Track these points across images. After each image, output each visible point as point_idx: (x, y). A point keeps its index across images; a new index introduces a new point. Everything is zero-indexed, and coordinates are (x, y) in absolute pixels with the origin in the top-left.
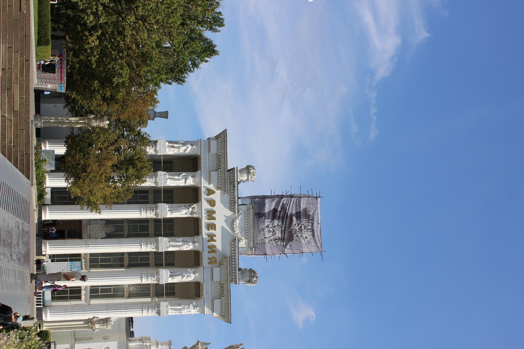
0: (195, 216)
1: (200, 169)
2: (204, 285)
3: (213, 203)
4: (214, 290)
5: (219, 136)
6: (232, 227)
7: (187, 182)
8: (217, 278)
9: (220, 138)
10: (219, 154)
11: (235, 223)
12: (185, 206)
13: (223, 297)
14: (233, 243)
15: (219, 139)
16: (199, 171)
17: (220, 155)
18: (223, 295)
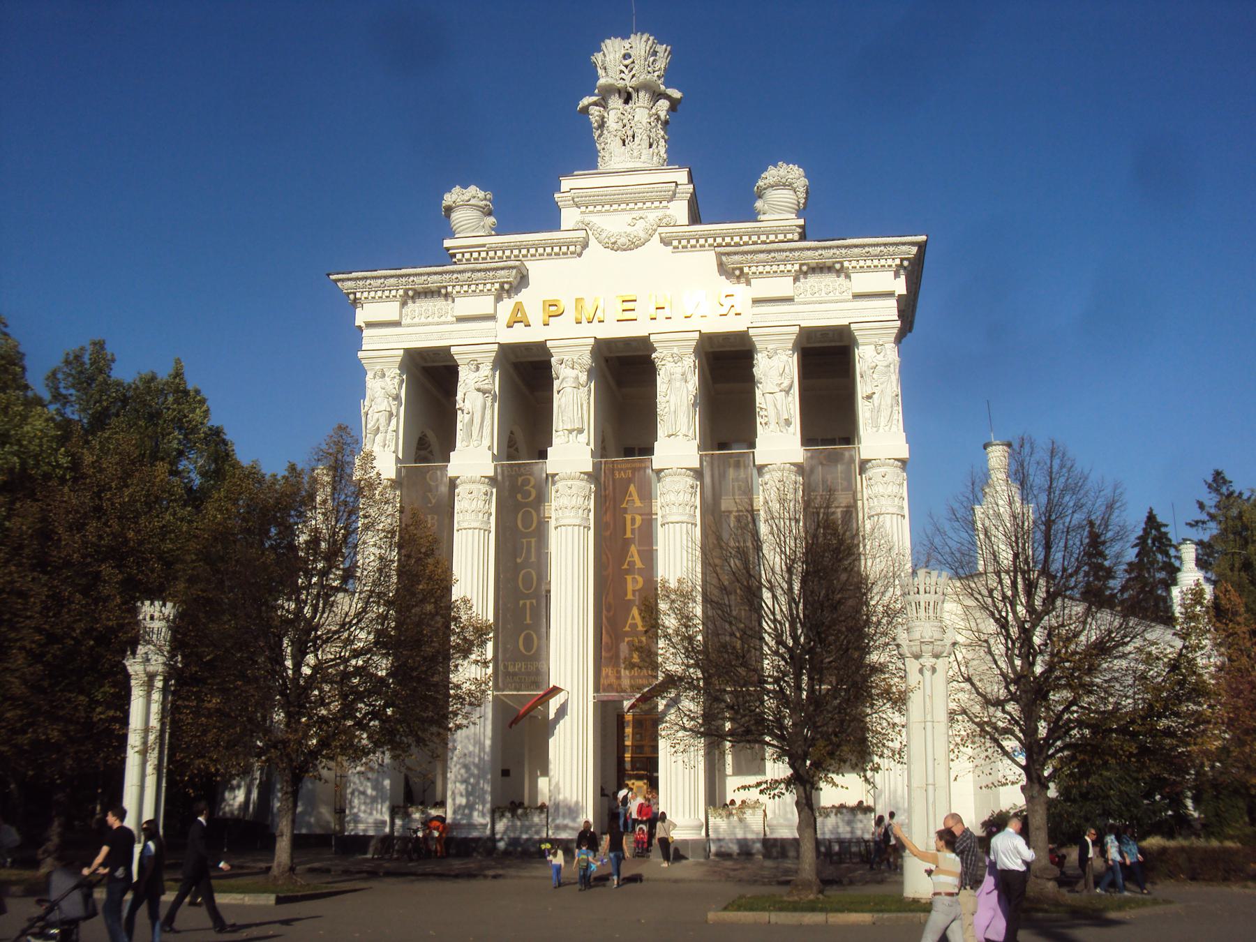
0: (587, 360)
1: (447, 350)
2: (804, 324)
3: (552, 308)
4: (823, 294)
5: (352, 296)
6: (625, 250)
7: (486, 387)
8: (782, 286)
9: (355, 294)
10: (401, 292)
11: (613, 240)
12: (559, 392)
13: (842, 263)
14: (675, 243)
15: (358, 295)
16: (453, 350)
17: (406, 291)
18: (838, 266)
